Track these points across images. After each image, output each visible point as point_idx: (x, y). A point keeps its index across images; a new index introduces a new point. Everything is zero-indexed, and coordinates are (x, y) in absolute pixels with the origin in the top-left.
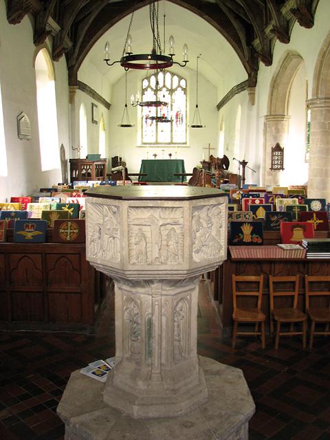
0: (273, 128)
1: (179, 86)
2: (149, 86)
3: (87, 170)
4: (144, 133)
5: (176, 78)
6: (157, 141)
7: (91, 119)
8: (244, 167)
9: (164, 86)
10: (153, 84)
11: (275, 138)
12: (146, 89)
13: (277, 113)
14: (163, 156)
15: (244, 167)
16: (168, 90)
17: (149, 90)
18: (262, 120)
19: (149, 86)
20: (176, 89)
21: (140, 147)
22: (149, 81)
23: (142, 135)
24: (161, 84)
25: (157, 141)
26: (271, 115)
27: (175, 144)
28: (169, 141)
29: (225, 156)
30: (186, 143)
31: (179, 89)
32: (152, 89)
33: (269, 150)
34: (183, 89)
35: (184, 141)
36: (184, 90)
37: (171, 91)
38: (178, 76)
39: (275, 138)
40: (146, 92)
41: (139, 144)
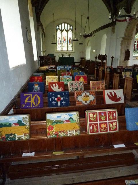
0: (126, 42)
1: (70, 29)
2: (59, 29)
5: (69, 26)
6: (62, 50)
8: (112, 59)
9: (65, 29)
10: (60, 28)
11: (127, 47)
12: (58, 30)
13: (129, 36)
14: (66, 55)
15: (112, 59)
16: (66, 30)
17: (59, 30)
18: (121, 39)
19: (59, 29)
20: (69, 30)
21: (56, 52)
24: (63, 28)
25: (62, 50)
26: (125, 37)
28: (67, 50)
29: (105, 55)
30: (72, 51)
31: (70, 30)
32: (60, 30)
34: (71, 30)
35: (72, 50)
36: (72, 31)
37: (67, 31)
38: (70, 25)
39: (127, 47)
40: (58, 31)
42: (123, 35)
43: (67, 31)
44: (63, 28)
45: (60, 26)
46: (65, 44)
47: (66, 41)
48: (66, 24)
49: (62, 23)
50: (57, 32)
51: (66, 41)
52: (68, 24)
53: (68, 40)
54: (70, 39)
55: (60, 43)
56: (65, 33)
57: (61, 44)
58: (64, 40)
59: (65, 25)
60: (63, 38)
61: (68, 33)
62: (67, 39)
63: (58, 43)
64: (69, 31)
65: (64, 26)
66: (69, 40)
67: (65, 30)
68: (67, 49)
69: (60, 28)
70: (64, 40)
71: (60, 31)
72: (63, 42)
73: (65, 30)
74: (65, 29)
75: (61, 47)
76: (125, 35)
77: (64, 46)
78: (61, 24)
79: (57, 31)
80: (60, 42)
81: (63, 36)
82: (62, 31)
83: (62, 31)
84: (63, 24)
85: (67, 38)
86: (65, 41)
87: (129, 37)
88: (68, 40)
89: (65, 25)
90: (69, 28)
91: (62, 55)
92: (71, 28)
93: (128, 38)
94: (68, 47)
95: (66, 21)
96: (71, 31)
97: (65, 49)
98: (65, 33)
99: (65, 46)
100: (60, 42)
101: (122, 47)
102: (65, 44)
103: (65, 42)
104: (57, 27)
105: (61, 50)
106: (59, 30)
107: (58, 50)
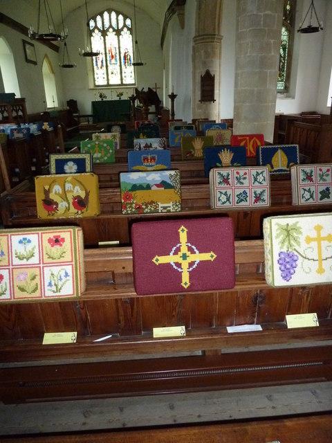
1: (125, 25)
2: (96, 27)
3: (17, 111)
4: (96, 76)
5: (121, 17)
6: (108, 82)
7: (23, 57)
8: (173, 101)
9: (111, 26)
10: (100, 25)
11: (205, 63)
12: (93, 31)
13: (206, 32)
15: (173, 101)
16: (114, 30)
17: (96, 31)
18: (192, 44)
20: (122, 29)
22: (95, 22)
23: (94, 79)
24: (107, 25)
25: (108, 82)
26: (199, 36)
27: (126, 85)
31: (125, 29)
32: (99, 29)
33: (198, 79)
34: (129, 29)
37: (118, 32)
38: (123, 15)
39: (205, 63)
40: (94, 34)
41: (92, 86)
42: (193, 35)
43: (118, 32)
44: (107, 25)
45: (99, 18)
46: (114, 68)
47: (116, 60)
48: (113, 14)
50: (91, 35)
51: (116, 60)
52: (118, 14)
53: (122, 56)
54: (126, 53)
55: (102, 65)
57: (104, 68)
58: (112, 57)
59: (110, 16)
60: (107, 52)
61: (121, 37)
63: (97, 65)
64: (122, 33)
65: (101, 22)
66: (125, 57)
67: (111, 30)
68: (122, 79)
69: (100, 25)
70: (112, 57)
71: (100, 34)
72: (108, 62)
73: (111, 30)
74: (111, 26)
75: (106, 77)
76: (197, 30)
77: (112, 73)
78: (101, 15)
79: (90, 33)
80: (102, 62)
81: (107, 46)
82: (104, 33)
83: (104, 33)
84: (106, 15)
85: (118, 52)
86: (114, 60)
87: (207, 35)
88: (122, 56)
89: (110, 16)
90: (121, 25)
91: (101, 96)
92: (128, 22)
93: (203, 39)
94: (123, 75)
95: (114, 5)
96: (129, 32)
97: (115, 80)
98: (111, 36)
99: (115, 72)
100: (102, 62)
101: (194, 67)
102: (114, 68)
103: (113, 61)
104: (92, 23)
105: (105, 83)
106: (96, 31)
107: (97, 84)
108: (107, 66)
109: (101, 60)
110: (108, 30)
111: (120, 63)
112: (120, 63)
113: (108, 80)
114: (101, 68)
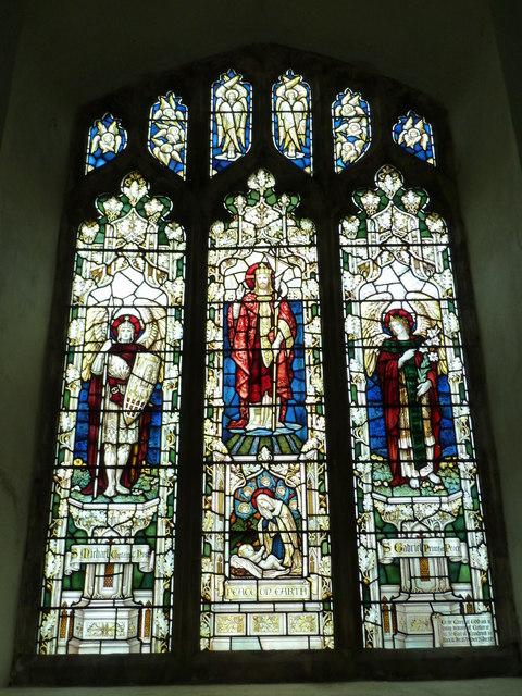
1: (384, 152)
2: (136, 160)
5: (349, 105)
9: (263, 152)
10: (169, 140)
16: (289, 180)
19: (136, 160)
20: (361, 176)
43: (325, 197)
45: (168, 109)
47: (292, 406)
49: (212, 77)
51: (292, 406)
53: (359, 366)
54: (391, 348)
56: (261, 245)
62: (335, 348)
63: (89, 446)
66: (388, 382)
68: (346, 598)
69: (169, 140)
74: (263, 152)
77: (243, 532)
79: (81, 196)
81: (225, 288)
82: (198, 199)
83: (198, 199)
84: (231, 98)
88: (359, 366)
100: (148, 418)
108: (192, 464)
109: (136, 393)
110: (235, 180)
111: (339, 430)
112: (339, 430)
113: (188, 601)
114: (129, 475)
